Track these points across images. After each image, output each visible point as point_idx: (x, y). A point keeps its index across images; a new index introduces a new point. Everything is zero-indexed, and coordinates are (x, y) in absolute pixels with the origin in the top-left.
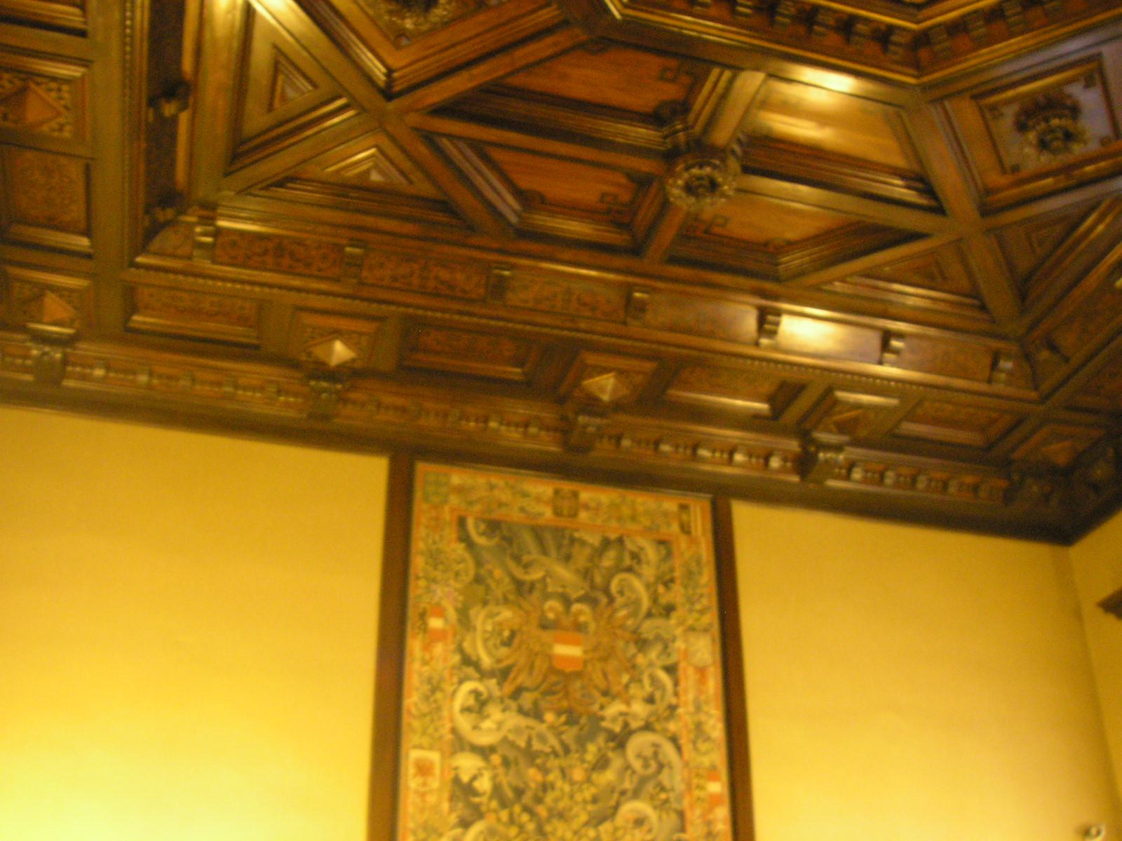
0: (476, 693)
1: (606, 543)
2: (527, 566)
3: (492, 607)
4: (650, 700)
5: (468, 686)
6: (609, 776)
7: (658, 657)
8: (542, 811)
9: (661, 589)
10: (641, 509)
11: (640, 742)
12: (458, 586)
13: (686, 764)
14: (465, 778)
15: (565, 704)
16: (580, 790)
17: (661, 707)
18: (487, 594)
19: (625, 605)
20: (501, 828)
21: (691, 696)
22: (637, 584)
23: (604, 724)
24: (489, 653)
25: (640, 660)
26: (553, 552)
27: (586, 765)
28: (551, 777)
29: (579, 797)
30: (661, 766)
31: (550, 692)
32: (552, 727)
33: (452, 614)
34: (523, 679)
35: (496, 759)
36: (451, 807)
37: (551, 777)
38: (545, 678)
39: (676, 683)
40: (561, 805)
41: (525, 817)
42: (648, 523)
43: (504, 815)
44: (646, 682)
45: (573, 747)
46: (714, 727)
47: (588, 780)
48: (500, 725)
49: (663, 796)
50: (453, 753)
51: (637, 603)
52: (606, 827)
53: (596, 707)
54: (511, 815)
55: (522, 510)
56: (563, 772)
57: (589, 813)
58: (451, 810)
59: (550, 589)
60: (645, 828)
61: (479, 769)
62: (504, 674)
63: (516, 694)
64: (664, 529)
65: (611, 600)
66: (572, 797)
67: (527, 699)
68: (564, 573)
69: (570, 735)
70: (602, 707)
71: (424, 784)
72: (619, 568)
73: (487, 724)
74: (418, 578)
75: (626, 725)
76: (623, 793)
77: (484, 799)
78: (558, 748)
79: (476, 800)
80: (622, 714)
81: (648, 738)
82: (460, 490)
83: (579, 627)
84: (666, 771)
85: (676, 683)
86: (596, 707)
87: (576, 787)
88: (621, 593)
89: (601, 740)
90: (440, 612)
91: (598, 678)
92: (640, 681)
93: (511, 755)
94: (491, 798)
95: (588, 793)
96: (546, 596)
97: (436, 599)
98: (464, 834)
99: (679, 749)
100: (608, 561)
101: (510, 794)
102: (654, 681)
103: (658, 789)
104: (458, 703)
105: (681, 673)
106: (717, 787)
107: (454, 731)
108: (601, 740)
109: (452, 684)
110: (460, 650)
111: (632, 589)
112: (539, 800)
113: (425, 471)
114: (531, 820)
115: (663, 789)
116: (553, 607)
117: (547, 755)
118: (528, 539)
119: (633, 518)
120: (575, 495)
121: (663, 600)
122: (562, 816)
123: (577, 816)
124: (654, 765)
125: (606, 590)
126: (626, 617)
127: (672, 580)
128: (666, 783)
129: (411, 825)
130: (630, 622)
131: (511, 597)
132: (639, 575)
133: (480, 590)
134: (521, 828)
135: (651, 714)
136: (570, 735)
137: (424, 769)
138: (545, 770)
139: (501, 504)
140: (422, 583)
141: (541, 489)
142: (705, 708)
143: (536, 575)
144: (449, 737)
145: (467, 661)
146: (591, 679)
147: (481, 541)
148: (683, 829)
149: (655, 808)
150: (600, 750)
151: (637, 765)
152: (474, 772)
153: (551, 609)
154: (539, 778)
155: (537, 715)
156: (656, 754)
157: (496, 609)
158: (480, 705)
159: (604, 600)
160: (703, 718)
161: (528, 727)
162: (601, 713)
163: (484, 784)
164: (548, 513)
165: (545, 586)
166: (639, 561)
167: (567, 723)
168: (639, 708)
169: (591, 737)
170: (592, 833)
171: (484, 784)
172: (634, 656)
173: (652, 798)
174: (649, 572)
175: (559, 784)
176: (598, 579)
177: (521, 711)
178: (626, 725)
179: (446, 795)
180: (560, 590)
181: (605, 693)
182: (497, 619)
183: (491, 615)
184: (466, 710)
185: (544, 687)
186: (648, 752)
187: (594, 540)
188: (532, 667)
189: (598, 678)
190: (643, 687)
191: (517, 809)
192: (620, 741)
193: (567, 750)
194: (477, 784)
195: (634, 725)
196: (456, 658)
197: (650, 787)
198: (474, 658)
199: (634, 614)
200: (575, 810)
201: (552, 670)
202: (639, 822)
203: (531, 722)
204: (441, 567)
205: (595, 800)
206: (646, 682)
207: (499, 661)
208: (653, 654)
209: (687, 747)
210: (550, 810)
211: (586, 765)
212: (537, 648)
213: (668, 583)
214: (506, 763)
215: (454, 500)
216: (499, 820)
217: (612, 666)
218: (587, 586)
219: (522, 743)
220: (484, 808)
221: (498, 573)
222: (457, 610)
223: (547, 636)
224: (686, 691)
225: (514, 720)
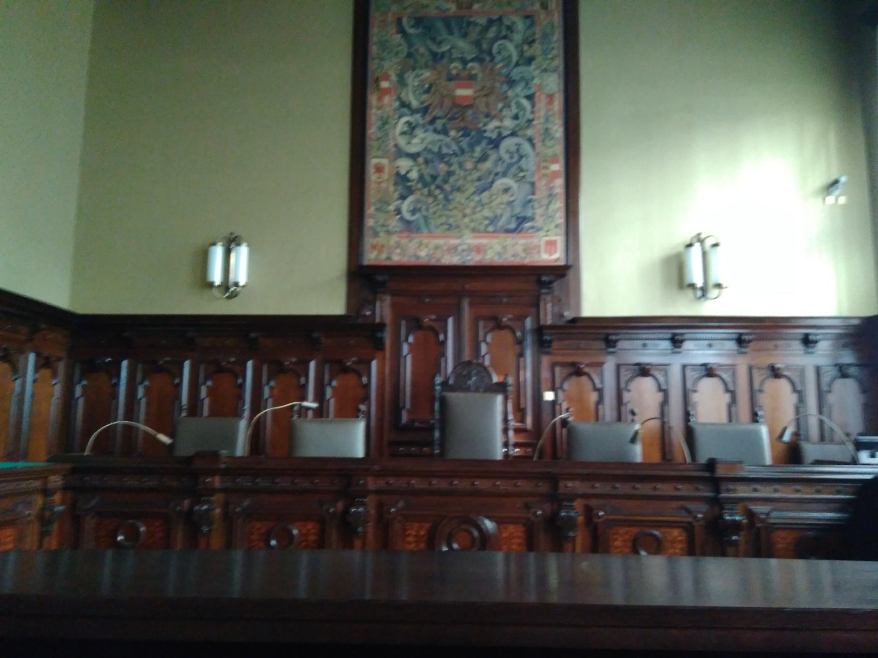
2: (439, 43)
3: (418, 71)
4: (516, 117)
6: (488, 165)
7: (522, 90)
8: (447, 187)
11: (508, 144)
13: (537, 155)
14: (403, 172)
15: (462, 124)
16: (470, 174)
17: (522, 121)
19: (502, 61)
21: (542, 113)
23: (487, 134)
25: (510, 93)
26: (456, 31)
28: (453, 168)
30: (521, 157)
31: (452, 119)
34: (437, 112)
35: (421, 160)
37: (453, 168)
38: (450, 110)
39: (533, 106)
40: (460, 183)
41: (437, 192)
43: (425, 191)
45: (467, 149)
46: (557, 131)
47: (475, 168)
48: (423, 140)
49: (522, 174)
50: (396, 159)
52: (486, 194)
53: (481, 125)
55: (437, 8)
56: (461, 165)
57: (476, 187)
58: (395, 191)
59: (454, 56)
60: (510, 193)
61: (412, 166)
62: (425, 110)
67: (439, 124)
68: (462, 44)
69: (465, 143)
70: (485, 125)
71: (379, 178)
75: (500, 134)
76: (497, 174)
78: (458, 151)
79: (409, 184)
83: (472, 77)
84: (524, 159)
85: (533, 106)
86: (481, 125)
89: (484, 143)
91: (482, 108)
92: (509, 107)
93: (430, 156)
94: (418, 182)
95: (475, 175)
96: (452, 60)
98: (402, 203)
99: (533, 145)
100: (491, 33)
101: (428, 179)
102: (519, 105)
103: (519, 170)
105: (536, 99)
106: (558, 167)
111: (505, 49)
112: (446, 181)
115: (522, 170)
116: (455, 67)
118: (440, 25)
122: (459, 189)
123: (467, 189)
124: (516, 157)
125: (490, 52)
128: (524, 167)
129: (373, 200)
130: (504, 71)
131: (430, 63)
134: (435, 197)
135: (516, 126)
136: (465, 143)
137: (379, 169)
138: (449, 164)
142: (552, 119)
143: (445, 48)
144: (393, 150)
148: (533, 193)
149: (517, 181)
150: (482, 150)
151: (506, 157)
152: (408, 169)
153: (455, 68)
155: (445, 132)
156: (518, 150)
158: (412, 129)
159: (488, 58)
160: (550, 125)
161: (439, 141)
162: (485, 128)
163: (414, 175)
165: (451, 54)
167: (462, 136)
168: (508, 123)
169: (478, 142)
170: (477, 198)
171: (414, 175)
172: (506, 91)
173: (515, 176)
175: (458, 171)
176: (485, 46)
177: (436, 131)
178: (500, 134)
179: (392, 183)
180: (460, 56)
181: (487, 116)
182: (422, 77)
184: (403, 133)
185: (449, 116)
186: (514, 149)
187: (482, 21)
188: (441, 104)
190: (511, 110)
192: (495, 144)
193: (463, 151)
194: (409, 175)
197: (513, 170)
199: (507, 65)
200: (467, 186)
202: (506, 190)
203: (441, 137)
205: (479, 179)
208: (519, 89)
209: (539, 145)
210: (452, 186)
211: (474, 160)
212: (445, 93)
214: (427, 162)
216: (422, 194)
217: (492, 99)
219: (436, 149)
220: (413, 188)
221: (422, 50)
223: (452, 84)
225: (431, 137)
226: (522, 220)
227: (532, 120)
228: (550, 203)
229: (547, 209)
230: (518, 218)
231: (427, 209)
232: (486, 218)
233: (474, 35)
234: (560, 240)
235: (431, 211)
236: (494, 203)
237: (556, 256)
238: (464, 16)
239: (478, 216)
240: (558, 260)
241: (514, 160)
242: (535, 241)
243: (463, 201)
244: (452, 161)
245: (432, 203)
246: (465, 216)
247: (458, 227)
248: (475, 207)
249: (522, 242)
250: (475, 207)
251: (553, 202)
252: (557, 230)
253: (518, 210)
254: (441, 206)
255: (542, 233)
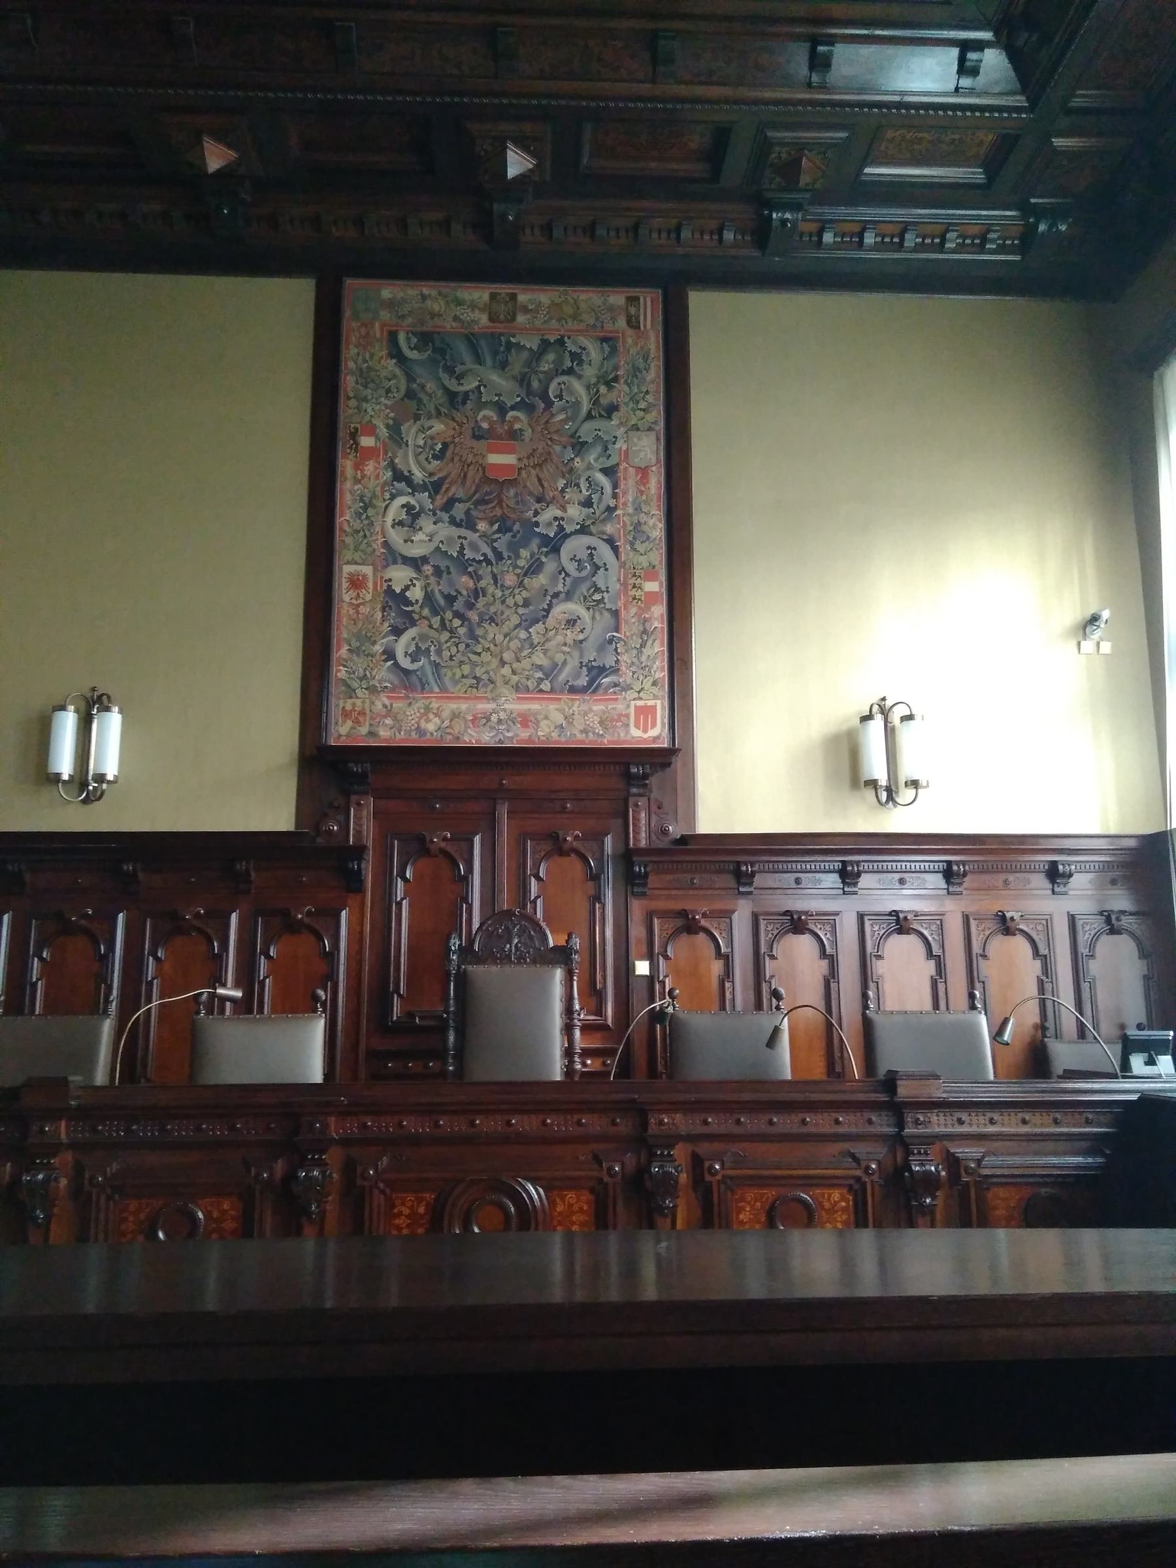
0: (408, 507)
1: (545, 345)
2: (459, 378)
4: (588, 503)
5: (402, 500)
6: (542, 579)
7: (596, 460)
8: (473, 616)
9: (603, 389)
10: (583, 306)
11: (575, 546)
12: (389, 403)
13: (623, 565)
15: (498, 512)
17: (599, 509)
18: (418, 410)
19: (564, 409)
20: (433, 633)
22: (579, 387)
24: (424, 469)
25: (578, 463)
27: (518, 571)
28: (483, 583)
29: (510, 601)
32: (484, 535)
33: (383, 432)
34: (457, 491)
35: (428, 569)
36: (383, 616)
38: (478, 487)
39: (615, 486)
40: (493, 609)
41: (457, 622)
42: (592, 321)
44: (584, 485)
45: (505, 555)
48: (431, 537)
49: (597, 597)
50: (385, 567)
51: (577, 405)
52: (540, 627)
54: (443, 620)
57: (521, 616)
62: (435, 488)
63: (448, 506)
64: (609, 326)
65: (549, 404)
66: (503, 602)
67: (459, 510)
68: (500, 383)
69: (502, 543)
70: (536, 513)
72: (558, 371)
73: (420, 536)
74: (349, 398)
76: (556, 595)
77: (416, 608)
78: (491, 555)
80: (556, 519)
81: (585, 540)
82: (391, 304)
87: (507, 592)
88: (560, 397)
89: (534, 544)
90: (371, 431)
91: (532, 485)
92: (578, 485)
93: (443, 564)
94: (421, 607)
96: (481, 405)
97: (367, 418)
99: (616, 550)
101: (442, 602)
104: (389, 520)
107: (386, 544)
108: (534, 544)
109: (384, 500)
110: (392, 466)
112: (471, 606)
113: (353, 285)
114: (462, 626)
115: (597, 590)
117: (480, 562)
118: (462, 348)
119: (575, 317)
120: (513, 297)
121: (604, 401)
122: (492, 620)
125: (544, 396)
126: (565, 421)
127: (616, 379)
128: (601, 585)
132: (580, 377)
133: (412, 405)
135: (588, 517)
139: (433, 315)
140: (353, 403)
141: (479, 294)
143: (470, 384)
145: (398, 476)
146: (525, 487)
147: (413, 355)
150: (532, 555)
151: (571, 567)
154: (471, 584)
155: (471, 526)
156: (591, 555)
157: (427, 424)
161: (460, 537)
163: (416, 594)
164: (484, 319)
166: (581, 362)
168: (575, 512)
169: (525, 543)
170: (523, 635)
171: (416, 594)
174: (590, 372)
175: (491, 589)
176: (535, 384)
177: (453, 522)
178: (561, 528)
183: (422, 430)
186: (583, 554)
187: (533, 343)
189: (532, 485)
191: (449, 615)
192: (553, 545)
194: (408, 594)
195: (569, 529)
196: (389, 474)
197: (584, 589)
198: (406, 474)
199: (572, 418)
200: (507, 612)
201: (486, 480)
202: (571, 622)
203: (463, 532)
204: (371, 385)
205: (526, 603)
206: (584, 485)
207: (431, 474)
209: (624, 549)
210: (481, 615)
213: (611, 383)
214: (438, 572)
215: (385, 315)
218: (523, 395)
219: (455, 555)
220: (416, 617)
221: (430, 386)
222: (387, 426)
223: (481, 445)
224: (624, 493)
225: (445, 531)
226: (597, 672)
227: (615, 508)
228: (643, 645)
229: (640, 651)
230: (590, 669)
231: (439, 652)
232: (540, 668)
233: (518, 362)
234: (661, 707)
235: (446, 654)
236: (551, 645)
237: (653, 733)
238: (501, 334)
239: (526, 663)
240: (655, 739)
241: (584, 573)
242: (620, 707)
243: (499, 638)
244: (480, 572)
245: (446, 642)
246: (503, 663)
247: (492, 682)
248: (521, 650)
249: (598, 707)
250: (521, 650)
251: (649, 643)
252: (655, 690)
253: (591, 655)
254: (462, 647)
255: (631, 694)
